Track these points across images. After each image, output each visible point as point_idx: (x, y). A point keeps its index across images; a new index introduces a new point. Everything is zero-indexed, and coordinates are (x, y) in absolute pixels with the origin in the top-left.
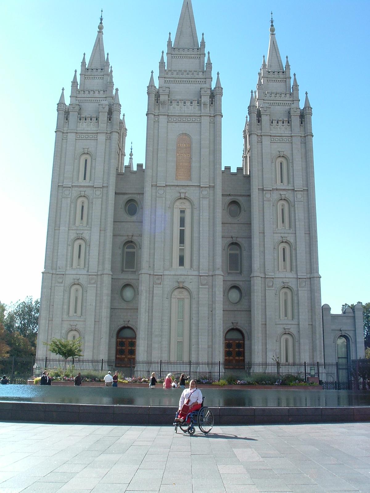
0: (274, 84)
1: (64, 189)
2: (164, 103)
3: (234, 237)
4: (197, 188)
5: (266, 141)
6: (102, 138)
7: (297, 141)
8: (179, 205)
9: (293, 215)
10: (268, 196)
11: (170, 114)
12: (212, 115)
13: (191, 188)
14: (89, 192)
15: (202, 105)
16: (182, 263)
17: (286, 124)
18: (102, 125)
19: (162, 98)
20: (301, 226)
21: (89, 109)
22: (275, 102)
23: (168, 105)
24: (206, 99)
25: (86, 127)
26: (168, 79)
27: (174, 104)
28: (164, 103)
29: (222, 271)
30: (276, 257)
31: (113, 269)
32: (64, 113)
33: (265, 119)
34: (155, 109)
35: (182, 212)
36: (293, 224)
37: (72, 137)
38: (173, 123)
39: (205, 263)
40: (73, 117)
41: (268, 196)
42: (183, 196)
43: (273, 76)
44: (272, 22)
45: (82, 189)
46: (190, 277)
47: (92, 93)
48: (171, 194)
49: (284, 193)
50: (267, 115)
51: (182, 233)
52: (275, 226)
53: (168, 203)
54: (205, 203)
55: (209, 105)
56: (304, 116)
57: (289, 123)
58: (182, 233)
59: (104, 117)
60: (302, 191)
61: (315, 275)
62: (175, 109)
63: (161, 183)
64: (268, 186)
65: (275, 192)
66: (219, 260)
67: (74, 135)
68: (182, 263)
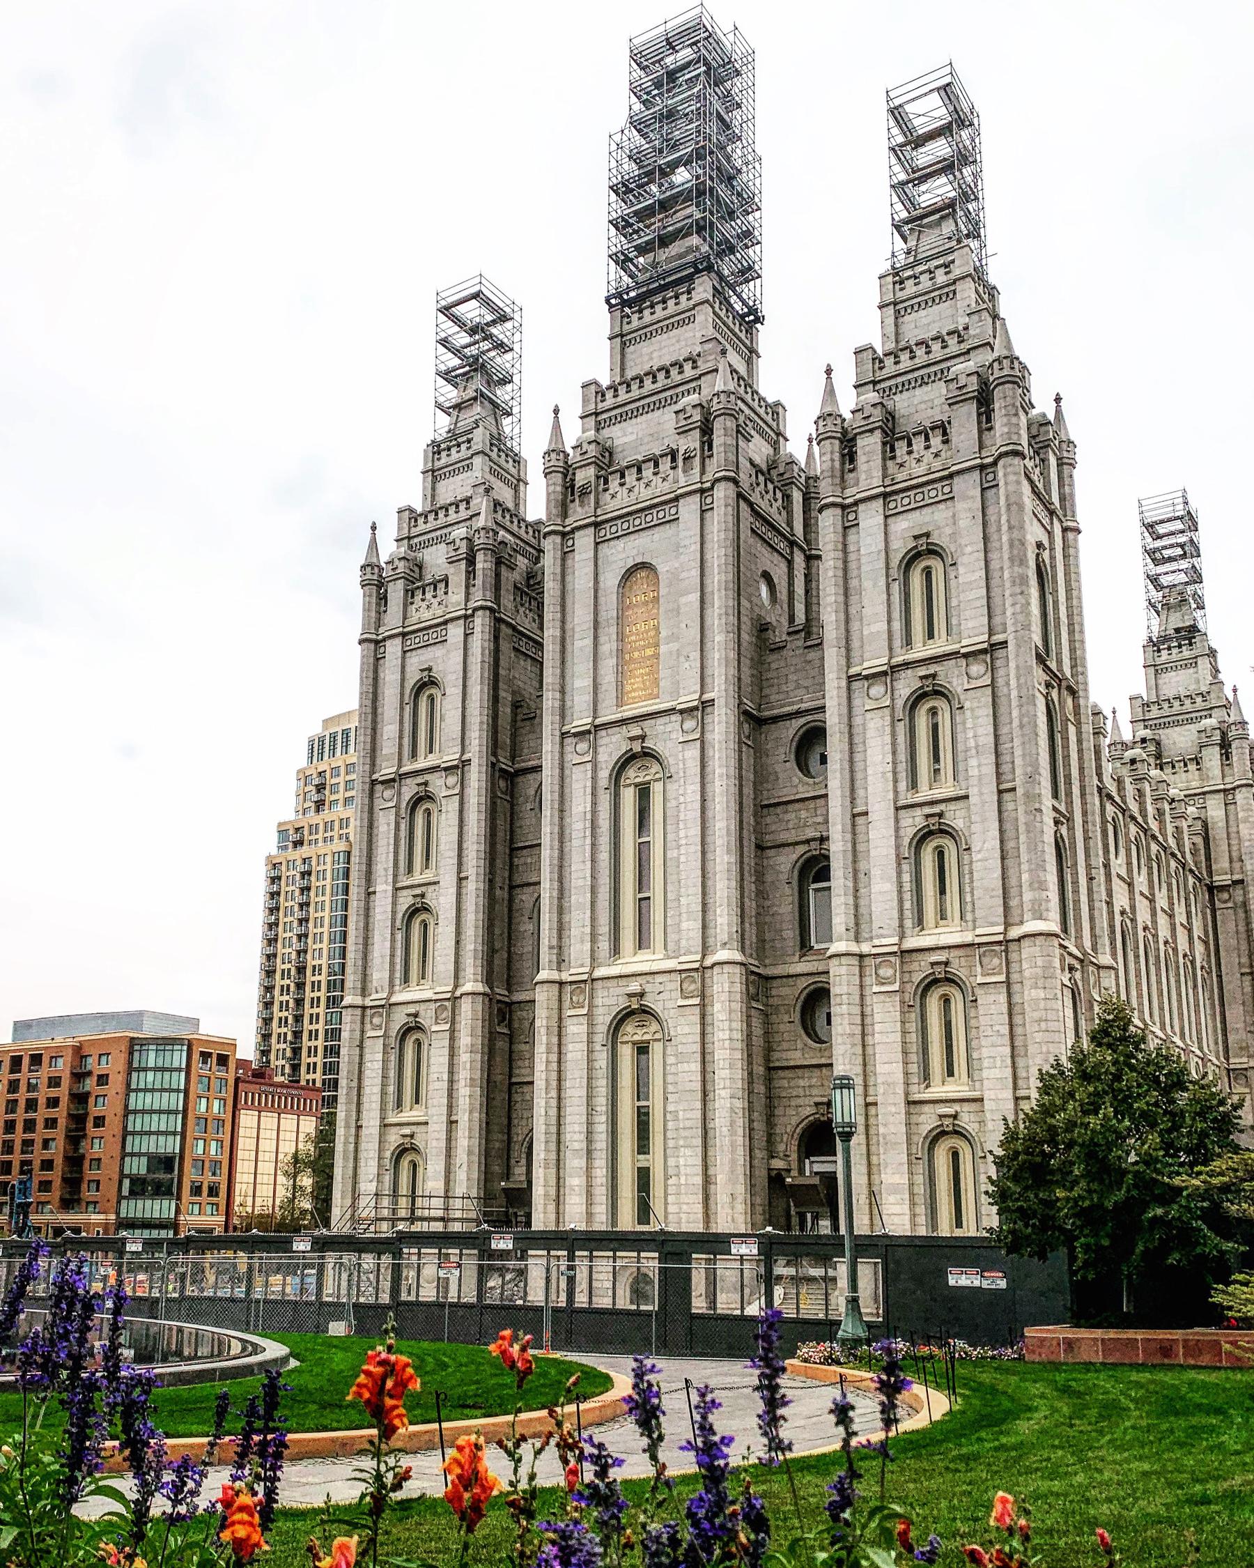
0: (922, 313)
2: (584, 493)
3: (814, 839)
4: (673, 718)
5: (871, 517)
6: (455, 632)
12: (708, 485)
13: (661, 721)
15: (680, 463)
17: (936, 441)
19: (584, 476)
21: (436, 559)
22: (910, 376)
23: (597, 494)
24: (692, 442)
26: (605, 416)
27: (614, 483)
29: (743, 950)
30: (907, 886)
32: (376, 582)
34: (565, 515)
39: (691, 927)
40: (396, 592)
41: (878, 690)
42: (637, 747)
43: (915, 289)
45: (420, 780)
46: (659, 978)
47: (441, 514)
48: (613, 746)
49: (932, 669)
50: (871, 431)
51: (643, 852)
52: (902, 786)
53: (604, 774)
54: (693, 752)
55: (698, 459)
57: (945, 433)
58: (643, 852)
59: (457, 575)
60: (984, 651)
62: (618, 498)
63: (581, 721)
66: (724, 920)
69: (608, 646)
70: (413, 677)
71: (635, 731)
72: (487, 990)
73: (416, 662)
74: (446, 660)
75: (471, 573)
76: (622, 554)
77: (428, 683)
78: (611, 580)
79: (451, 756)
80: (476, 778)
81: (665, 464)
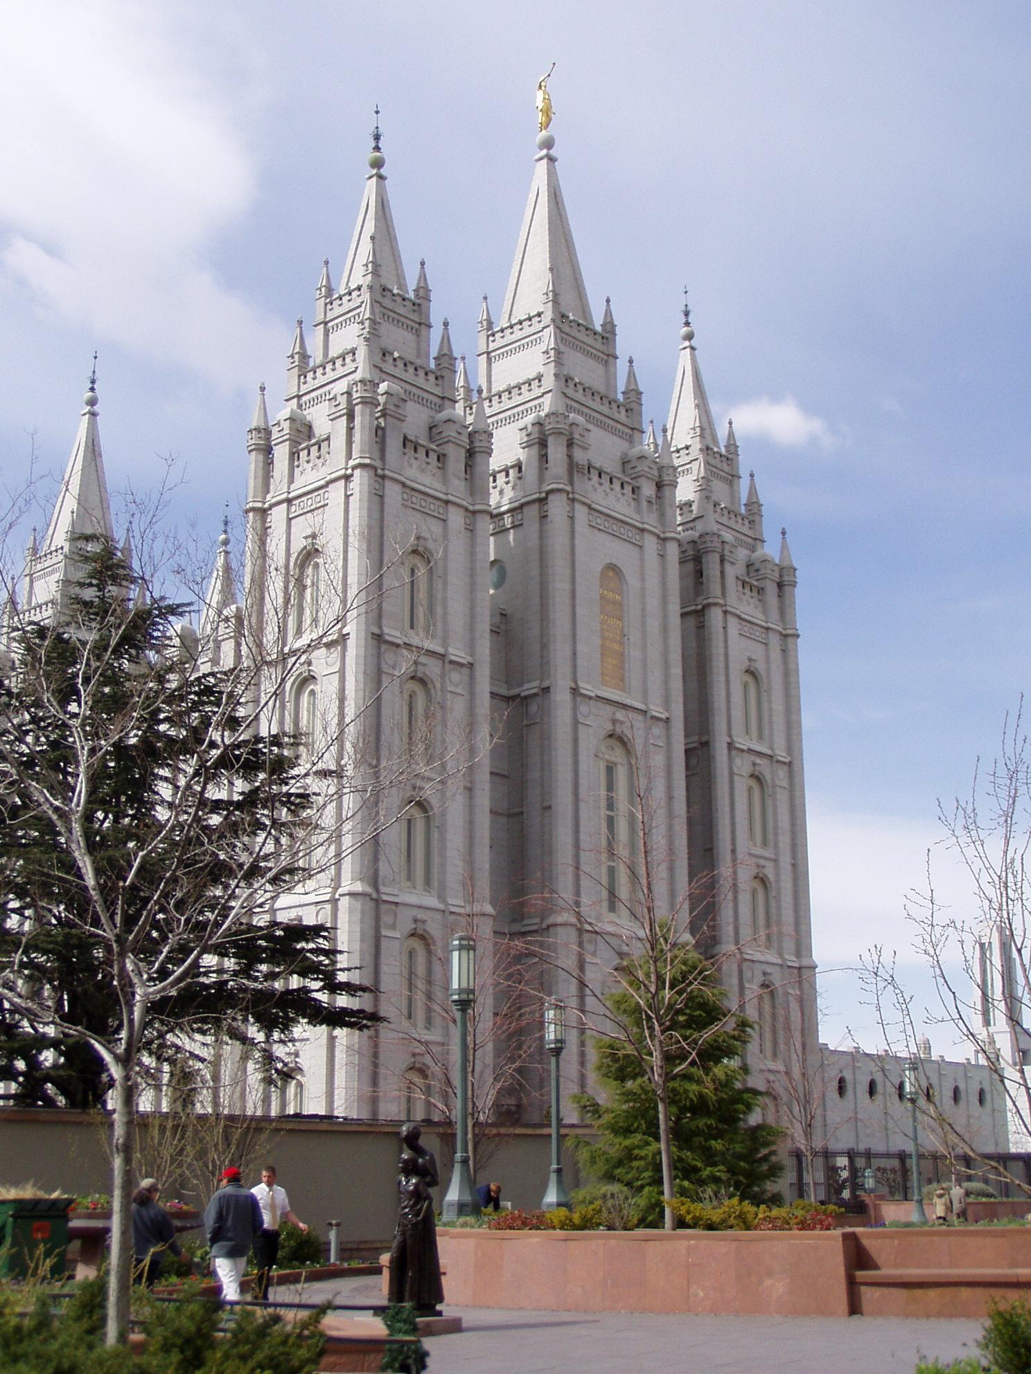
1: (384, 647)
4: (640, 717)
6: (456, 519)
7: (774, 640)
9: (770, 815)
10: (738, 761)
11: (594, 506)
14: (432, 669)
18: (455, 482)
20: (784, 840)
24: (648, 490)
33: (731, 571)
35: (610, 769)
36: (771, 837)
37: (393, 492)
38: (596, 532)
44: (687, 314)
54: (658, 760)
56: (784, 583)
61: (805, 962)
64: (742, 742)
65: (746, 755)
67: (398, 488)
72: (369, 890)
81: (628, 489)
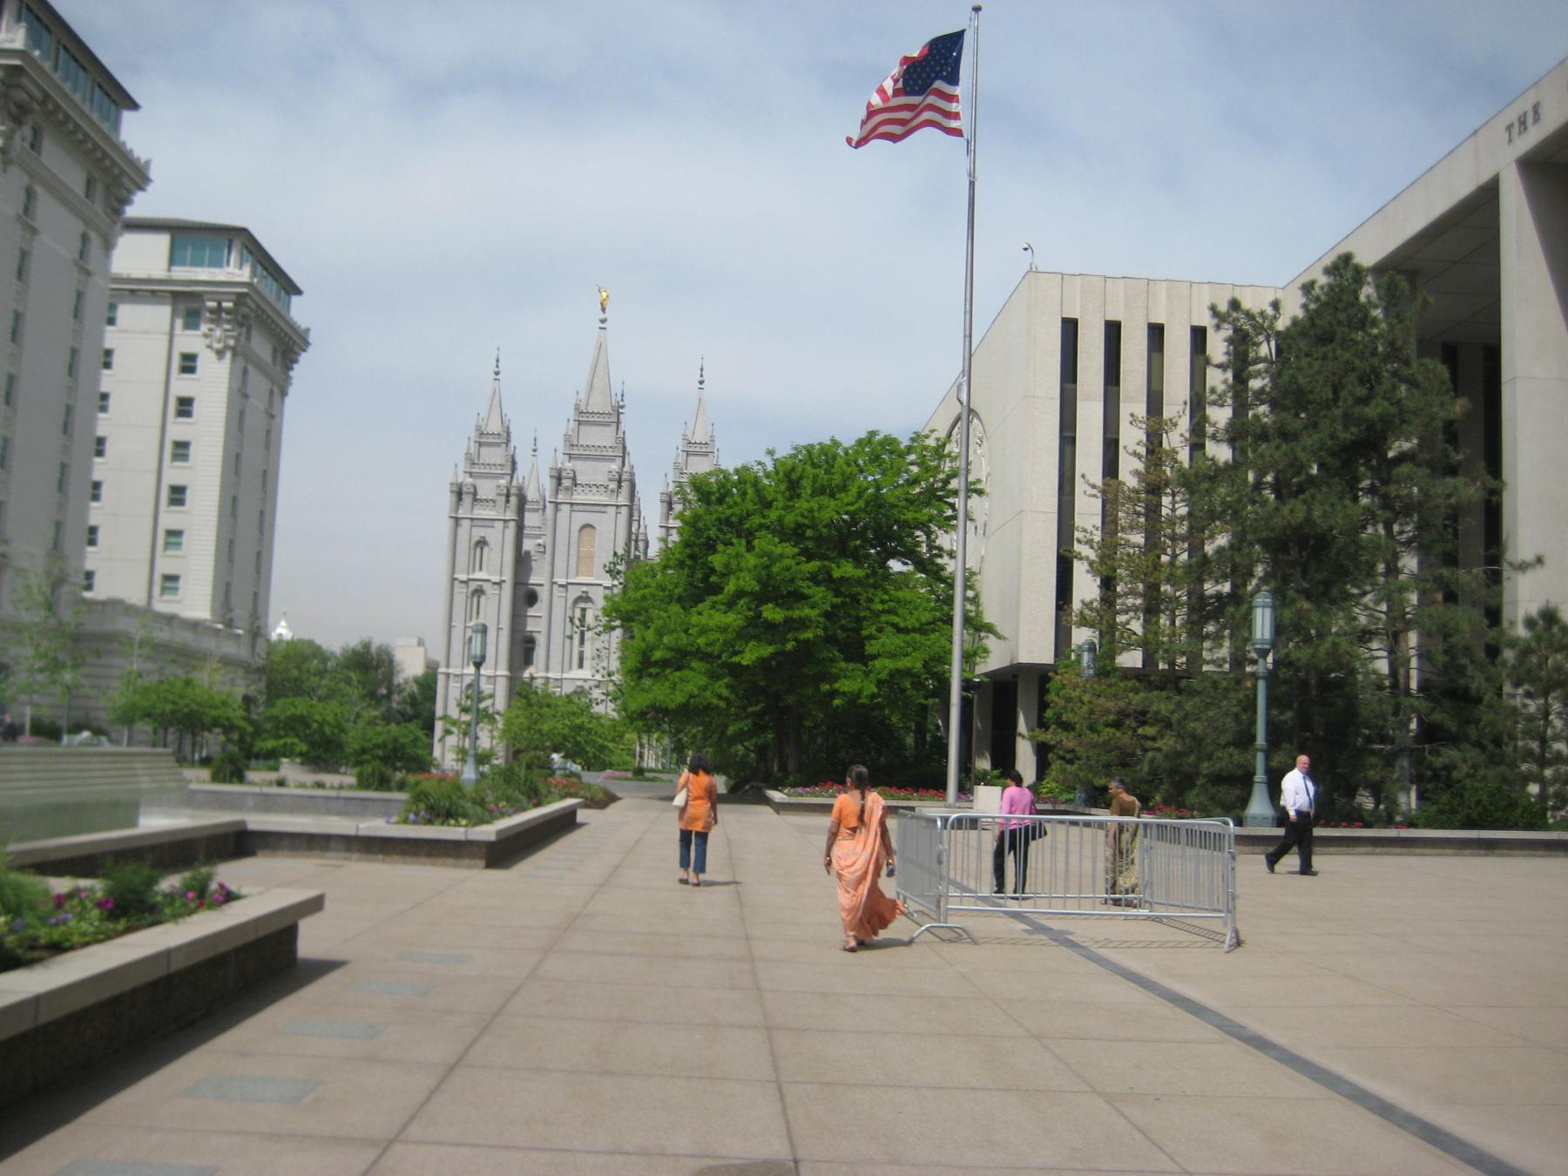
6: (499, 525)
8: (583, 605)
14: (486, 586)
16: (581, 666)
25: (480, 512)
27: (579, 489)
28: (567, 489)
31: (511, 668)
32: (459, 494)
35: (584, 610)
37: (465, 524)
40: (467, 500)
53: (570, 602)
62: (579, 497)
63: (563, 581)
68: (581, 666)
69: (573, 552)
70: (475, 539)
71: (585, 589)
73: (478, 533)
74: (493, 535)
75: (508, 501)
76: (581, 518)
77: (482, 543)
78: (576, 528)
79: (496, 579)
80: (507, 589)
